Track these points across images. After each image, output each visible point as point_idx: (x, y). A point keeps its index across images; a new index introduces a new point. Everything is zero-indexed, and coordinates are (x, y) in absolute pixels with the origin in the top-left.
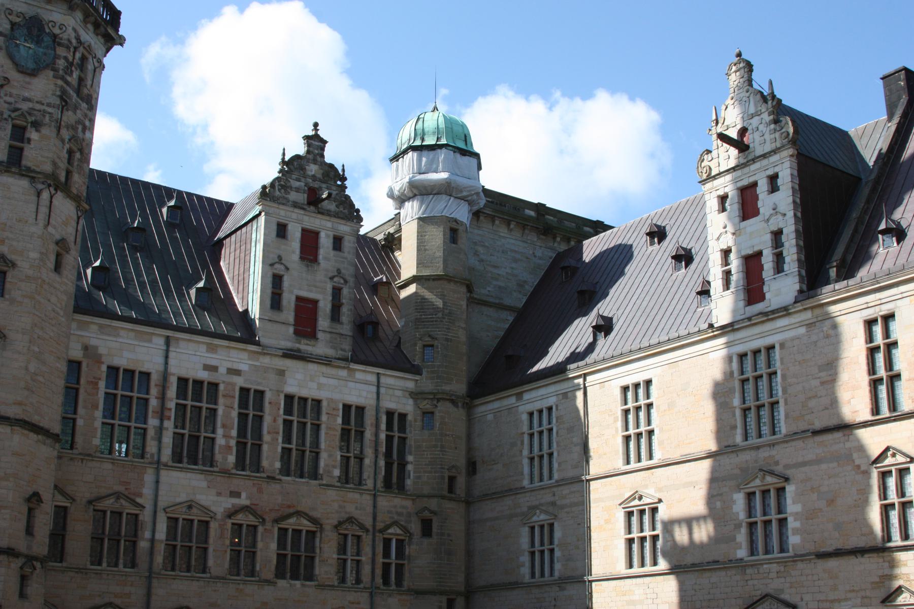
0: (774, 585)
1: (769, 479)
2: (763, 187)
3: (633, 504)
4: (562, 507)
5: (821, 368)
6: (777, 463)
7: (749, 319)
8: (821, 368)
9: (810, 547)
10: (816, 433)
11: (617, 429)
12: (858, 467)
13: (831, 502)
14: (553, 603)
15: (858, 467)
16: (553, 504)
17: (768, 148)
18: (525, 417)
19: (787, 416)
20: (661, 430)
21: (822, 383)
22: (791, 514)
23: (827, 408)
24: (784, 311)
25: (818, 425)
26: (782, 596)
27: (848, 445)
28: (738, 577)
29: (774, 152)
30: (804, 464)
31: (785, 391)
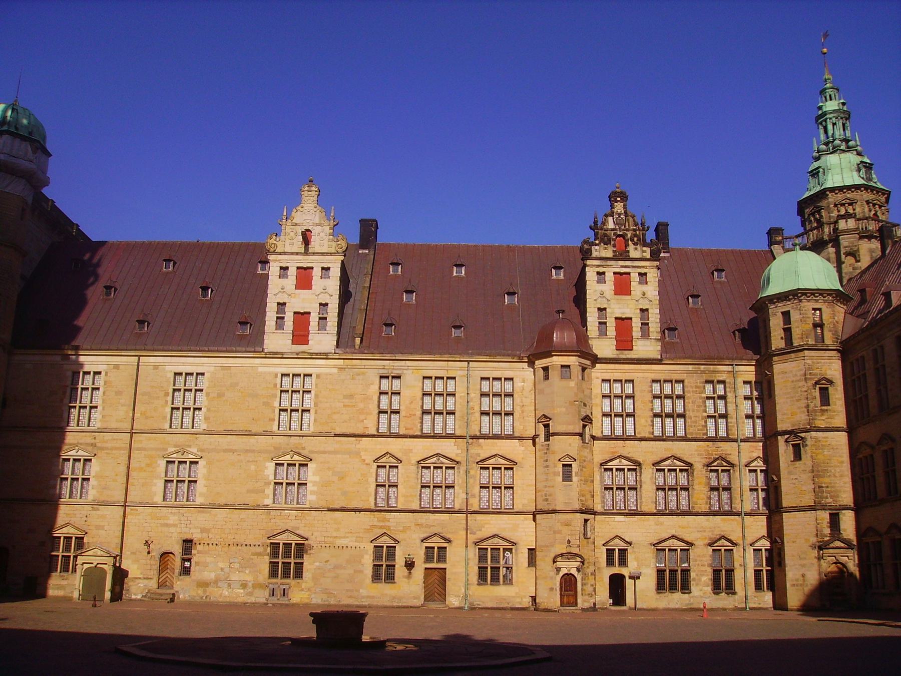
0: (290, 525)
1: (296, 457)
2: (317, 272)
3: (174, 456)
4: (102, 449)
5: (345, 397)
6: (304, 448)
7: (297, 354)
8: (345, 397)
9: (323, 504)
10: (336, 435)
11: (167, 402)
12: (364, 460)
13: (342, 478)
14: (85, 519)
15: (364, 460)
16: (94, 445)
17: (325, 250)
18: (69, 374)
19: (315, 420)
20: (208, 410)
21: (345, 406)
22: (311, 482)
23: (345, 422)
24: (325, 356)
25: (338, 432)
26: (297, 532)
27: (358, 446)
28: (264, 517)
29: (331, 254)
30: (324, 452)
31: (316, 405)
